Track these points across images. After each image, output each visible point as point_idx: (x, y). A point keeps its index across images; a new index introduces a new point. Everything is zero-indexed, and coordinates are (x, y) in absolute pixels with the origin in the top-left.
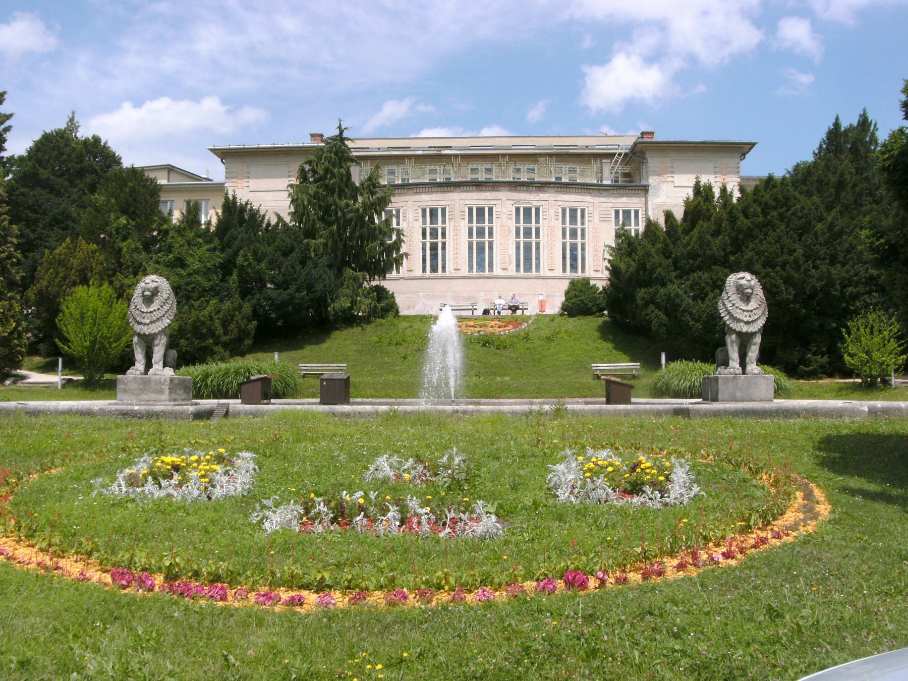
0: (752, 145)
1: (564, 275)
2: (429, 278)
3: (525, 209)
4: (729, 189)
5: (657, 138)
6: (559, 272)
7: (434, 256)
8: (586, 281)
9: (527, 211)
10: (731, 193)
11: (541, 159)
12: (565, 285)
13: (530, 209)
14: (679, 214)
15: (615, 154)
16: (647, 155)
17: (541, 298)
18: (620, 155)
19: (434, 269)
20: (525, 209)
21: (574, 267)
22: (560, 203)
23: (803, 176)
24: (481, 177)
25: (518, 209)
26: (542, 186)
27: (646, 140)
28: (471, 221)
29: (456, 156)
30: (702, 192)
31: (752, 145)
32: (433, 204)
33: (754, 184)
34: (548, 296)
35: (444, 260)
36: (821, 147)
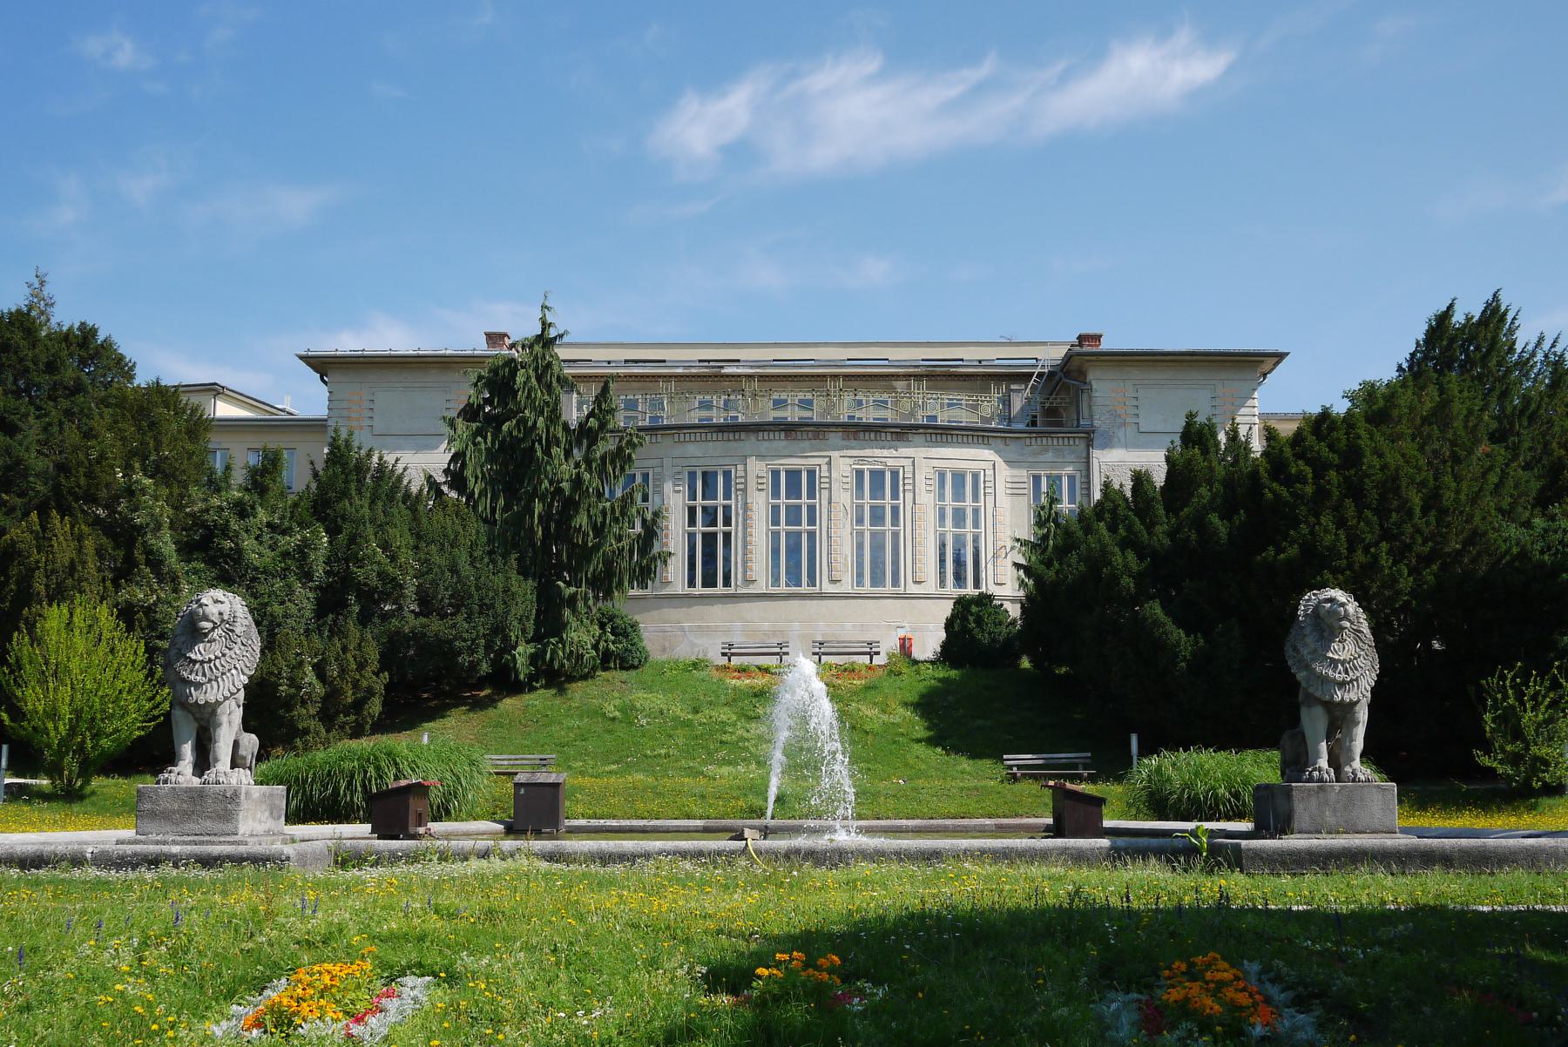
0: (1280, 356)
1: (941, 591)
2: (701, 596)
3: (872, 472)
4: (1243, 431)
5: (1105, 345)
6: (931, 587)
7: (711, 562)
8: (985, 600)
9: (877, 476)
10: (1248, 443)
11: (900, 385)
12: (946, 609)
13: (882, 473)
14: (1159, 478)
15: (1031, 375)
16: (1090, 377)
17: (901, 633)
18: (1040, 375)
19: (709, 581)
20: (872, 472)
21: (959, 578)
22: (936, 463)
23: (1375, 405)
24: (793, 414)
25: (860, 473)
26: (902, 433)
27: (1086, 349)
28: (776, 493)
29: (750, 377)
30: (1196, 436)
31: (1280, 356)
32: (709, 464)
33: (1294, 427)
34: (913, 630)
35: (727, 560)
36: (1413, 355)
